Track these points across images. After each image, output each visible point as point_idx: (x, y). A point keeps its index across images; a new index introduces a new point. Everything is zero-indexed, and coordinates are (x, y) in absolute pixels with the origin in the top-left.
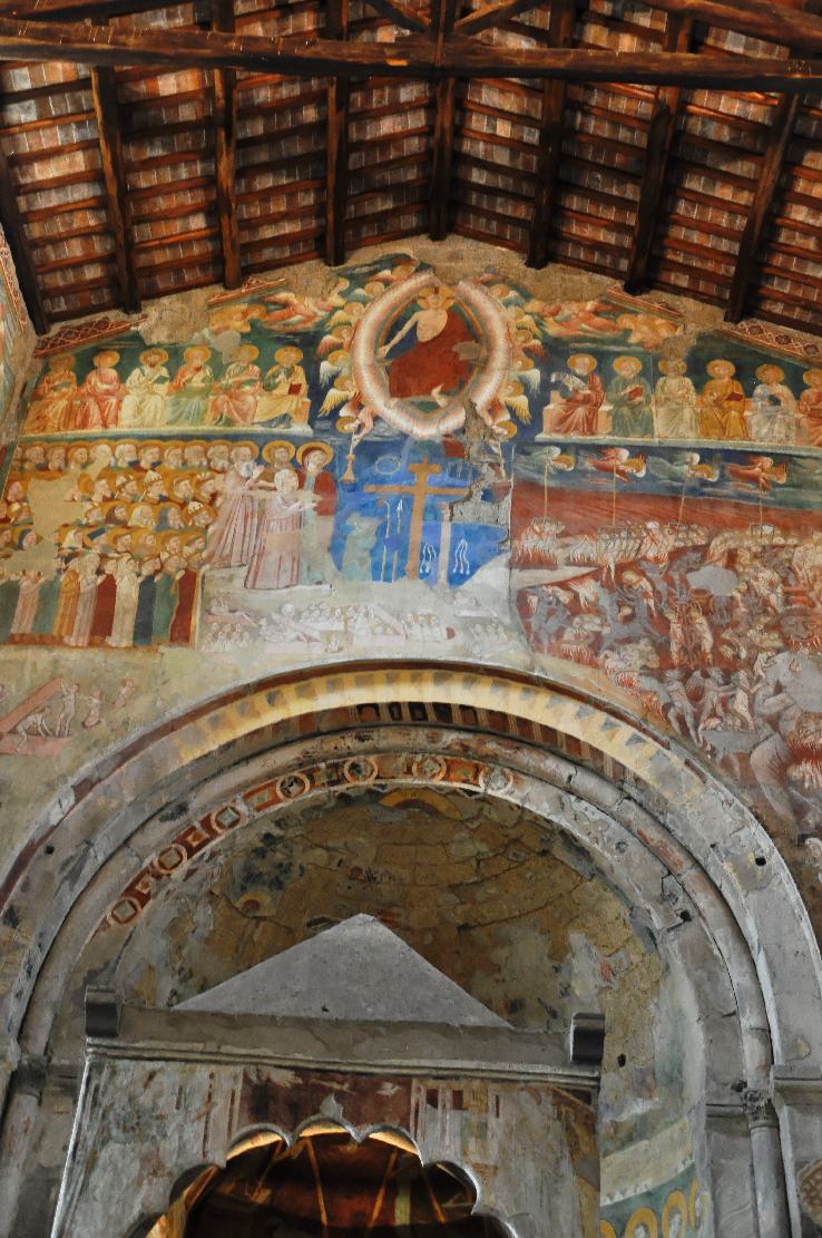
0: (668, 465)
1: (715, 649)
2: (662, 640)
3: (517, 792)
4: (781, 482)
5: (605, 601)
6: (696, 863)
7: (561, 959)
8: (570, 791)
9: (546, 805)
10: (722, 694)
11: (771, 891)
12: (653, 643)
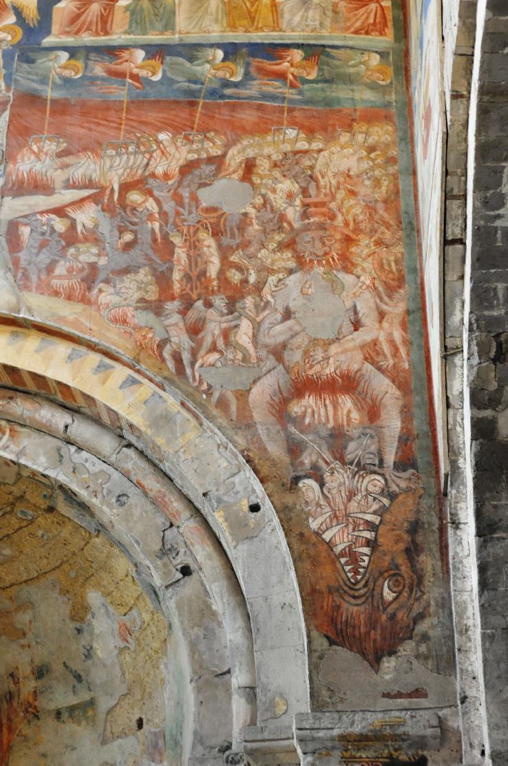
0: (188, 64)
1: (221, 272)
2: (164, 268)
3: (12, 446)
4: (311, 77)
5: (106, 228)
6: (197, 512)
7: (82, 620)
8: (69, 442)
9: (43, 459)
10: (224, 325)
11: (264, 539)
12: (154, 271)
